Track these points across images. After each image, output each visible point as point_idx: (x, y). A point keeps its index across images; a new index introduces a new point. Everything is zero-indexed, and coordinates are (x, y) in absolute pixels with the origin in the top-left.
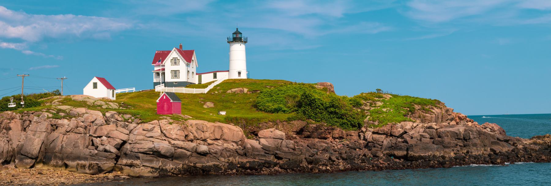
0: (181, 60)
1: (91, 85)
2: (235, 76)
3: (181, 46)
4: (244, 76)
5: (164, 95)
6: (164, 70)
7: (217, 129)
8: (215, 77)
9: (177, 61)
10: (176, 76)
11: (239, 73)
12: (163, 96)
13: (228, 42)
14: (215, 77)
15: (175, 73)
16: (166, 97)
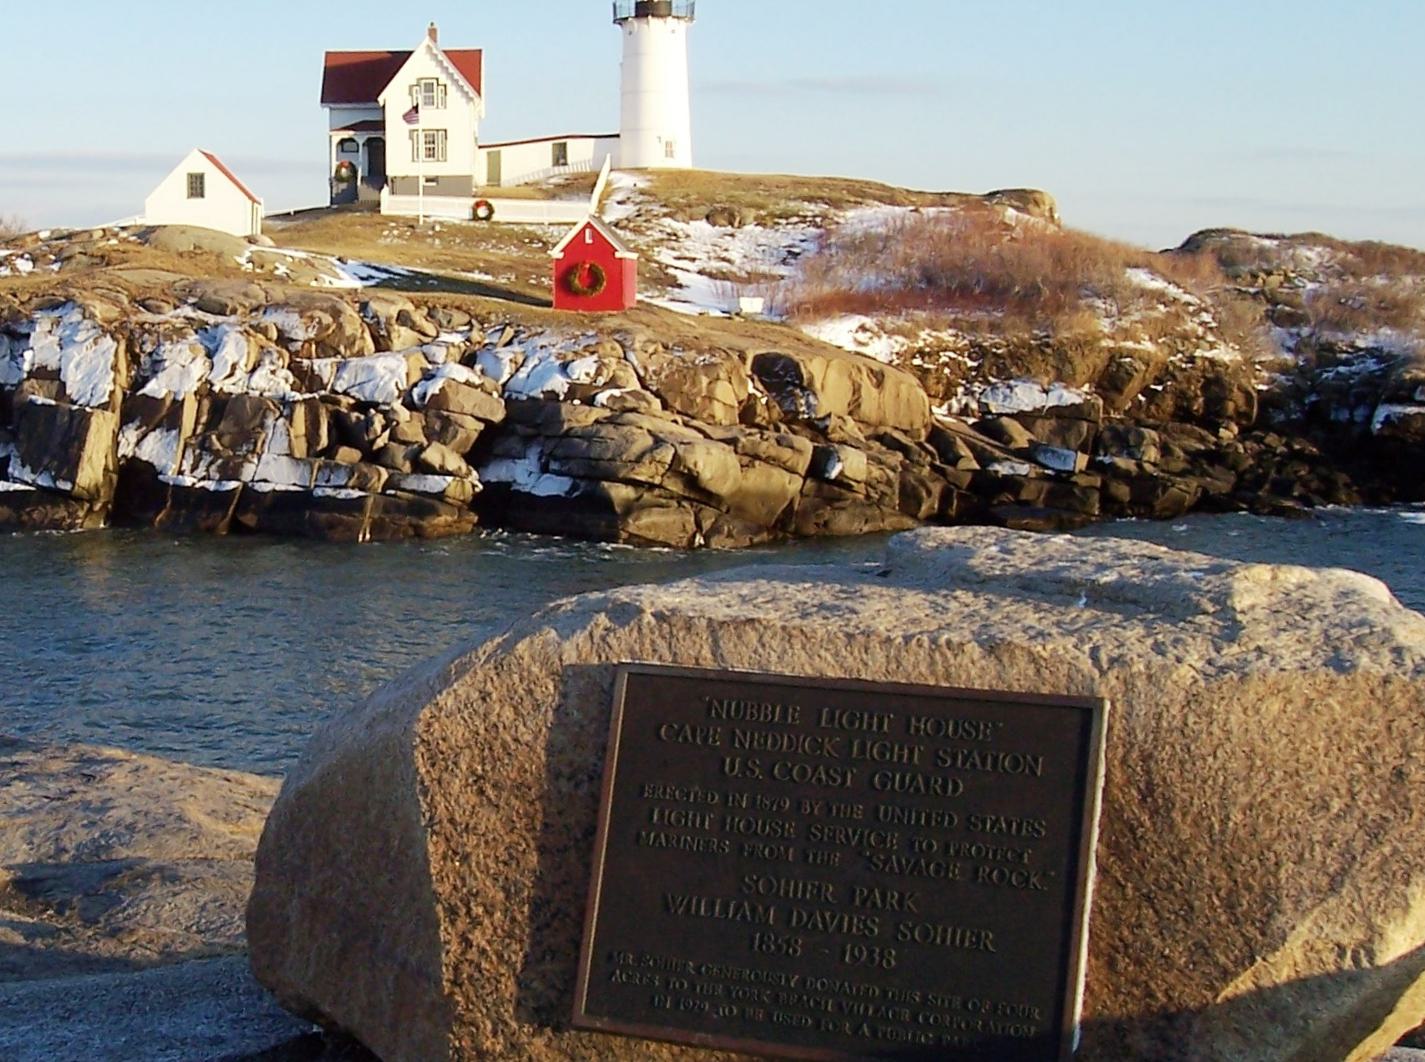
0: (451, 89)
1: (179, 182)
2: (655, 160)
3: (433, 33)
4: (683, 161)
5: (589, 225)
6: (380, 125)
7: (832, 374)
8: (560, 156)
9: (438, 93)
10: (431, 153)
11: (668, 144)
12: (583, 231)
13: (621, 21)
14: (560, 156)
15: (433, 144)
16: (596, 234)
